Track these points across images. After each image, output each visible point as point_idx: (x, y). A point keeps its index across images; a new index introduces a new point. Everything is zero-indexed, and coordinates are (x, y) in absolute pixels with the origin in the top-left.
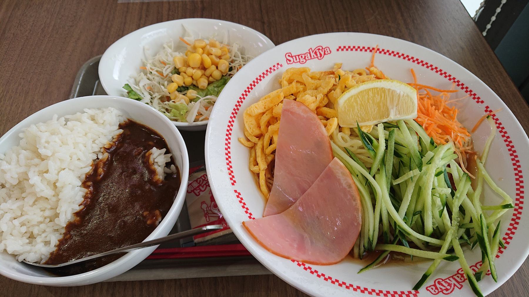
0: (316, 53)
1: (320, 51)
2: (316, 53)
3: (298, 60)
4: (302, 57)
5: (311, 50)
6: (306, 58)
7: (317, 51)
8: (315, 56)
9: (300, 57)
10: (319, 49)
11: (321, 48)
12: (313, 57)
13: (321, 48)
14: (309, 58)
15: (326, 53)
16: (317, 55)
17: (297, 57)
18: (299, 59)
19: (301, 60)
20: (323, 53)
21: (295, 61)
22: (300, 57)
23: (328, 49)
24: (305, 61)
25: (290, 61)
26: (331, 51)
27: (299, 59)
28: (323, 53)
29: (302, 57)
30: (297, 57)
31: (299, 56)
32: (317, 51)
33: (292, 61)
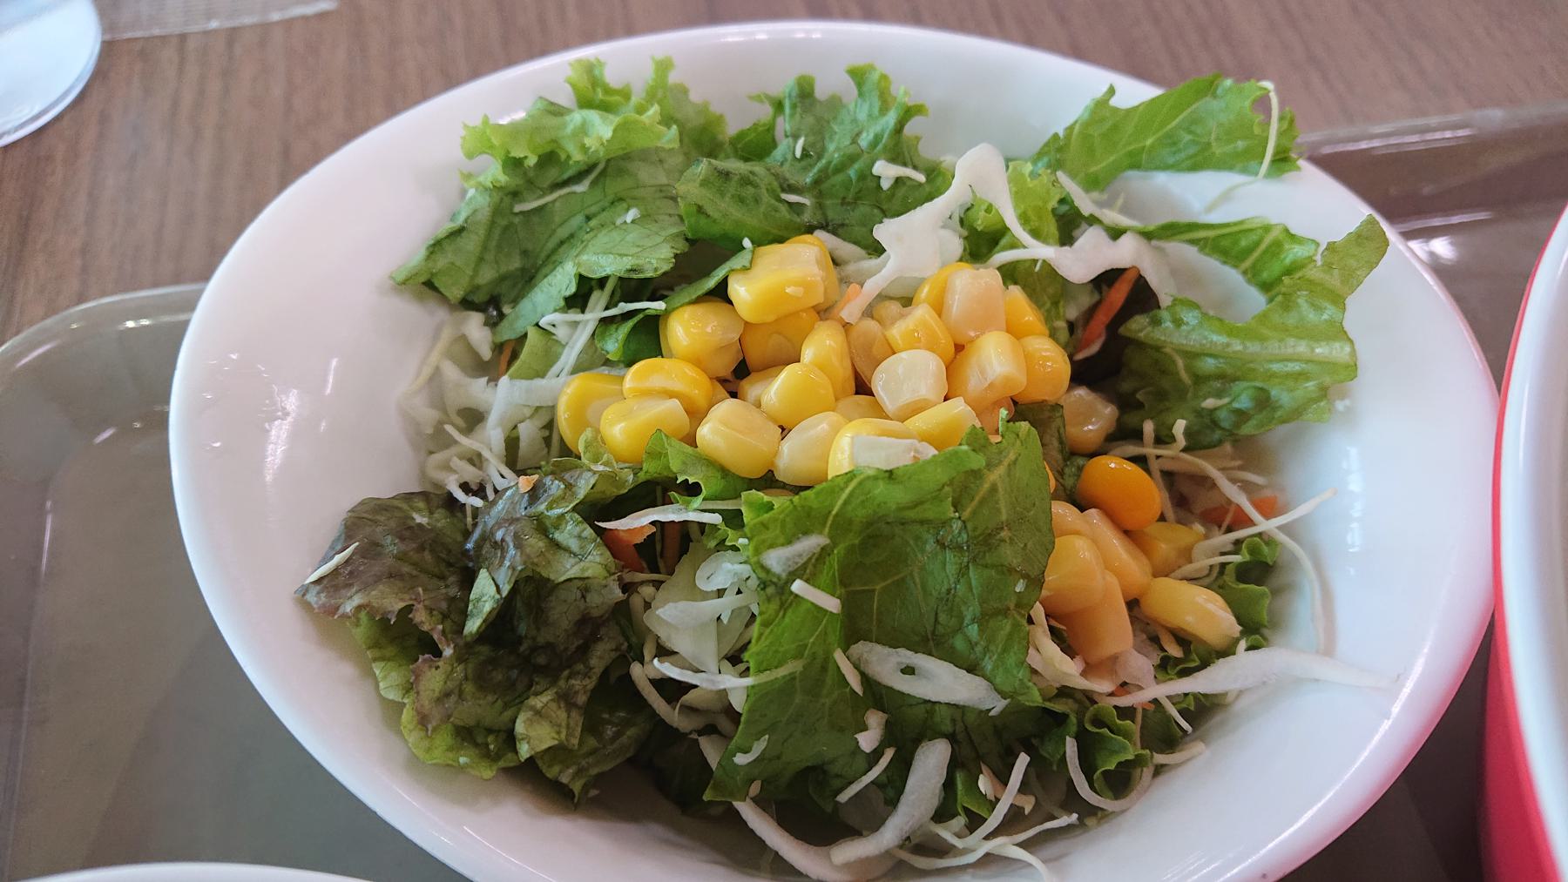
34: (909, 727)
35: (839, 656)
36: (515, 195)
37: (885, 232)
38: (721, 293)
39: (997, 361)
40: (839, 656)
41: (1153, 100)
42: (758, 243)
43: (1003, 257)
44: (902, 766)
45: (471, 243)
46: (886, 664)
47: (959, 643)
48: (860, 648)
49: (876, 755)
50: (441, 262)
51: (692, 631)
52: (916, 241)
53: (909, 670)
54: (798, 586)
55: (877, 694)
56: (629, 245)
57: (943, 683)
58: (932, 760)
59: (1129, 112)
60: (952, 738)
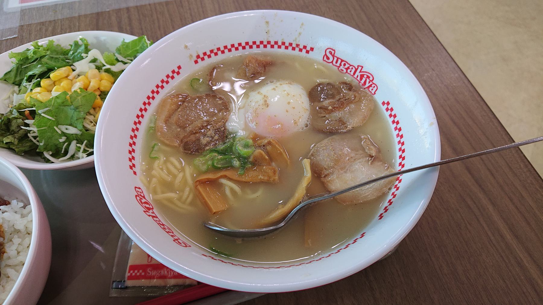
0: (362, 76)
1: (368, 80)
2: (362, 76)
3: (338, 64)
4: (345, 65)
5: (360, 68)
6: (349, 71)
7: (365, 76)
8: (359, 78)
9: (343, 63)
10: (368, 77)
11: (371, 79)
12: (355, 76)
13: (371, 79)
14: (352, 73)
15: (371, 88)
16: (361, 79)
17: (339, 61)
18: (340, 65)
19: (342, 67)
20: (367, 85)
21: (334, 62)
22: (343, 63)
23: (376, 88)
24: (345, 71)
25: (328, 58)
26: (375, 93)
27: (340, 65)
28: (367, 85)
29: (345, 65)
30: (339, 61)
31: (342, 61)
32: (365, 76)
33: (331, 60)
34: (69, 138)
35: (55, 127)
36: (22, 65)
37: (74, 64)
38: (49, 77)
39: (94, 84)
40: (55, 127)
41: (133, 41)
42: (58, 68)
43: (104, 68)
44: (69, 145)
45: (13, 74)
46: (63, 128)
47: (75, 125)
48: (59, 126)
49: (64, 142)
50: (7, 76)
51: (33, 127)
52: (81, 66)
53: (67, 129)
54: (42, 114)
55: (64, 134)
56: (37, 70)
57: (72, 130)
58: (74, 143)
59: (129, 43)
60: (77, 140)
